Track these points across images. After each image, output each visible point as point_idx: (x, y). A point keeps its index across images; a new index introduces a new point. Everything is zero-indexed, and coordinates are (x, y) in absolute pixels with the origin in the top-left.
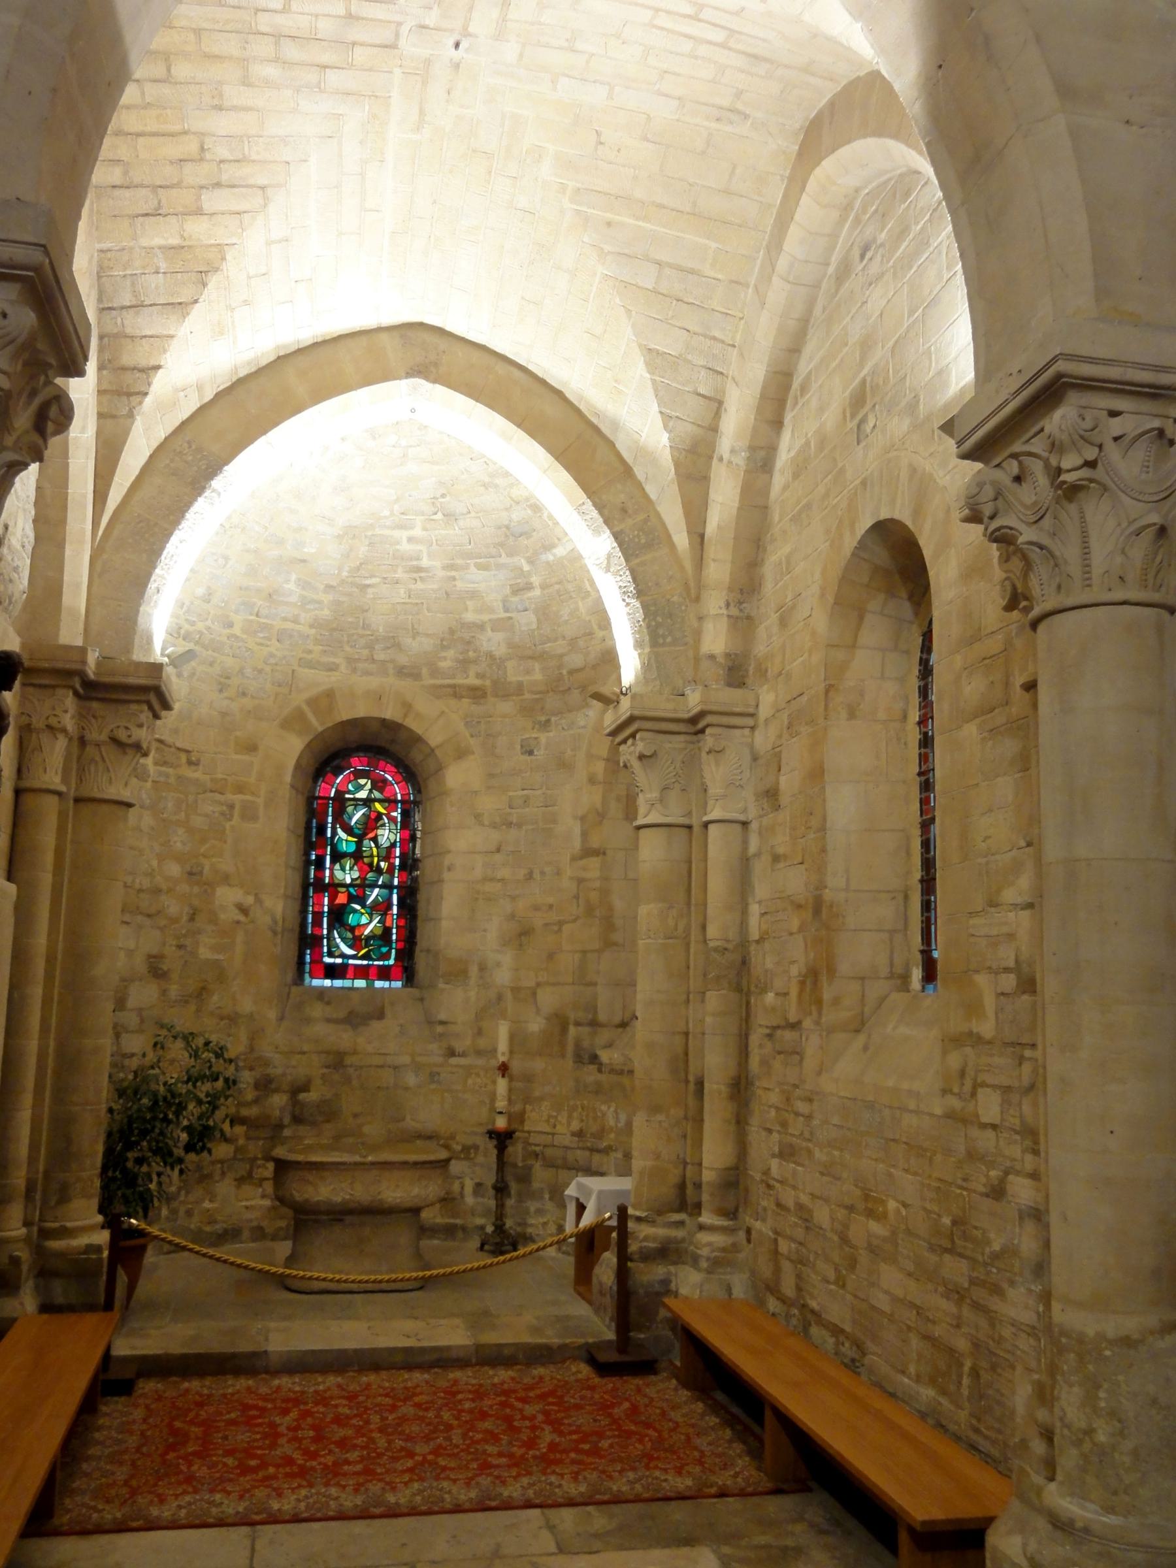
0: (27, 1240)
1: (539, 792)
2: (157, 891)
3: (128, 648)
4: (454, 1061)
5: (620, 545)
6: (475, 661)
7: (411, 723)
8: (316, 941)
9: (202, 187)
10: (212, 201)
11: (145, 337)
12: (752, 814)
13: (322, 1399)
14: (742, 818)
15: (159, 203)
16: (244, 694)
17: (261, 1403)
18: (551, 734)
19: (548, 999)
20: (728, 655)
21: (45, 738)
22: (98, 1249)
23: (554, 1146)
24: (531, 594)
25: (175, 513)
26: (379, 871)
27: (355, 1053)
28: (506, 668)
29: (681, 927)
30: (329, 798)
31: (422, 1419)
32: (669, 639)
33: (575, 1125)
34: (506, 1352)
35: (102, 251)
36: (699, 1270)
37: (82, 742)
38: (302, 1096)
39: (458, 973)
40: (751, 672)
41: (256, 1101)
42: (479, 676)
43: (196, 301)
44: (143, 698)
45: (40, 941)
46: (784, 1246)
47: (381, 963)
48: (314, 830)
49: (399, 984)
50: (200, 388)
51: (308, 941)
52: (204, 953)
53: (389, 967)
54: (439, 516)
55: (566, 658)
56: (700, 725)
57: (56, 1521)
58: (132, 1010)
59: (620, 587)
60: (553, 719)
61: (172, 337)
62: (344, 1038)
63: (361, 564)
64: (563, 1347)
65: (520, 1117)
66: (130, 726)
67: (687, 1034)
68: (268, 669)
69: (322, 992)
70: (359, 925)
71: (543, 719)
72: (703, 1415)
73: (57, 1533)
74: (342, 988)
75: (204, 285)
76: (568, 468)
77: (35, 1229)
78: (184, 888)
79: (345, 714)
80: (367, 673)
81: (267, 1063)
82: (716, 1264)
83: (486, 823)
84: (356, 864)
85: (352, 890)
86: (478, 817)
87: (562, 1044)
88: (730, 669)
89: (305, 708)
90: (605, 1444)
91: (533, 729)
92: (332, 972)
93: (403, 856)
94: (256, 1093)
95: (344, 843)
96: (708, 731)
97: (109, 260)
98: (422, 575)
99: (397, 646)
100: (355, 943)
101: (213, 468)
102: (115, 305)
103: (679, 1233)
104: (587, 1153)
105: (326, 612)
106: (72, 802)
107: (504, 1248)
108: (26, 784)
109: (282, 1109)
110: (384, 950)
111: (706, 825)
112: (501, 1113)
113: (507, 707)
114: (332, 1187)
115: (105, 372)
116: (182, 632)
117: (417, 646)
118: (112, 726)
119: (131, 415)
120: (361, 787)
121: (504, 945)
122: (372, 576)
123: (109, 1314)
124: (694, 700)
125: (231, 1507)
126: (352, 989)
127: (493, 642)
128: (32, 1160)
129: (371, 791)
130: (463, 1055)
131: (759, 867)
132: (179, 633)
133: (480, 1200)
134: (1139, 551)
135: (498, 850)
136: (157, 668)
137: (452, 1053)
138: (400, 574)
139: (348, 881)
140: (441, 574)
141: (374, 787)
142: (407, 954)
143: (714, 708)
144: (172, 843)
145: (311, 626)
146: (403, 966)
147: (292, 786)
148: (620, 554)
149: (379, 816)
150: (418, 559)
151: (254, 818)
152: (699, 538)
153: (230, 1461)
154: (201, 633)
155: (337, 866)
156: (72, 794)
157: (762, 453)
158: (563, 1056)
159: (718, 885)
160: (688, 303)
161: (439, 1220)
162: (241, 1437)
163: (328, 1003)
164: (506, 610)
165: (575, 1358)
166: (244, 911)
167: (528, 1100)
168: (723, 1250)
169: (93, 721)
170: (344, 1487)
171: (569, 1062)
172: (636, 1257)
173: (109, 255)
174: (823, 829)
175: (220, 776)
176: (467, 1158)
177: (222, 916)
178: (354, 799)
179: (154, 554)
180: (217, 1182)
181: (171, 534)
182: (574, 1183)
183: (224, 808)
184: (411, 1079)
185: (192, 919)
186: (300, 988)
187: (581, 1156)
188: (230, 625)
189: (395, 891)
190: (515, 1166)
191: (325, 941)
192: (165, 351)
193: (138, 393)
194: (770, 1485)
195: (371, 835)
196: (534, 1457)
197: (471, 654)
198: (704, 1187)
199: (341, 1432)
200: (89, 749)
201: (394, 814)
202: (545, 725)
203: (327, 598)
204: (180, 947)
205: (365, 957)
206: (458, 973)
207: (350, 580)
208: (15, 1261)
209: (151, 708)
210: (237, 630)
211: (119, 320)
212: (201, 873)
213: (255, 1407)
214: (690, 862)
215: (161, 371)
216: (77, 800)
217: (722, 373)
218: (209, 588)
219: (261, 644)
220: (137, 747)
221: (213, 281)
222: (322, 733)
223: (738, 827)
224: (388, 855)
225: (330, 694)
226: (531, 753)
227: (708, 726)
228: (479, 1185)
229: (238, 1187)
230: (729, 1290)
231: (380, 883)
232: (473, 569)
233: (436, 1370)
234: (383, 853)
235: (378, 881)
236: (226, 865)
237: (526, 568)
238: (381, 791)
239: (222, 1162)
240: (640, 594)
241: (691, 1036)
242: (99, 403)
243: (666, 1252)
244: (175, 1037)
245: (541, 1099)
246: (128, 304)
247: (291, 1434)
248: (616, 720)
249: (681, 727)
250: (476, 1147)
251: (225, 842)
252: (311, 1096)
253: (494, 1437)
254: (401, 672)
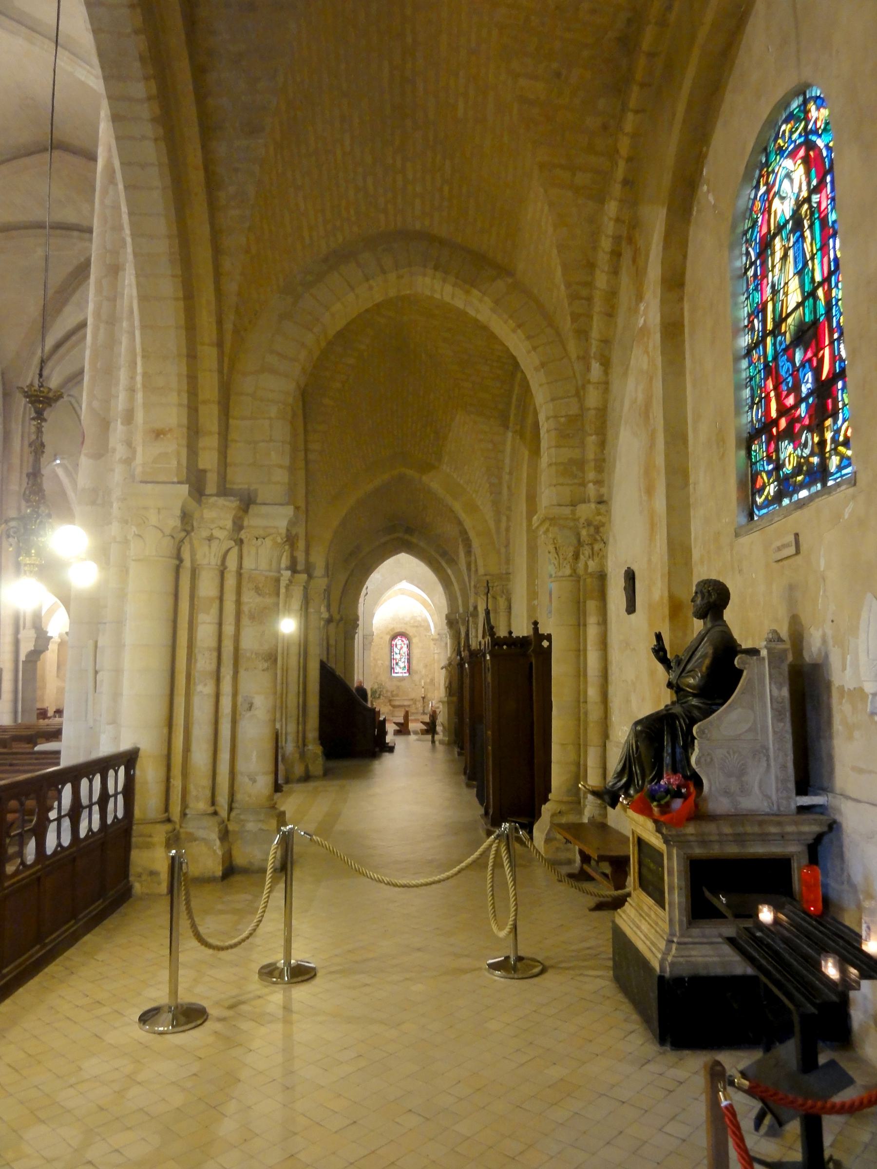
7: (407, 632)
8: (394, 668)
62: (399, 684)
92: (396, 673)
100: (400, 668)
137: (416, 685)
166: (382, 664)
206: (416, 672)
252: (394, 693)
254: (405, 624)
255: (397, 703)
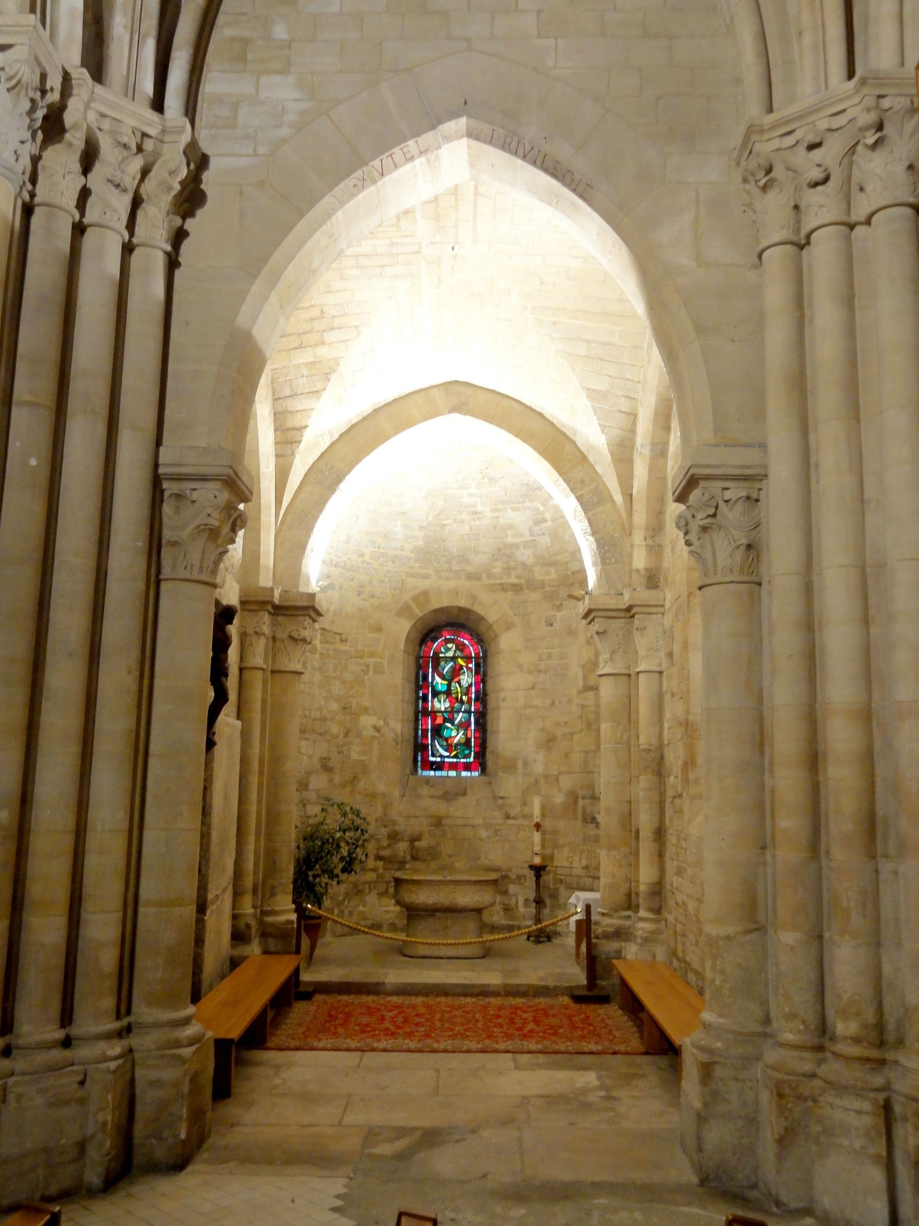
0: (254, 915)
1: (557, 650)
2: (324, 719)
3: (297, 585)
4: (510, 822)
5: (581, 504)
6: (514, 568)
7: (477, 609)
8: (424, 748)
9: (324, 331)
10: (329, 337)
11: (298, 411)
12: (664, 667)
13: (413, 1007)
14: (659, 669)
15: (302, 341)
16: (373, 596)
17: (379, 1007)
18: (564, 613)
19: (566, 782)
20: (646, 570)
21: (254, 639)
22: (292, 922)
23: (571, 875)
24: (545, 525)
25: (320, 505)
26: (462, 702)
27: (448, 817)
28: (534, 571)
29: (625, 737)
30: (430, 657)
31: (463, 1017)
32: (613, 560)
33: (584, 863)
34: (522, 989)
35: (273, 370)
36: (636, 943)
37: (274, 639)
38: (416, 843)
39: (511, 767)
40: (662, 579)
41: (389, 846)
42: (517, 577)
43: (325, 389)
44: (305, 613)
45: (255, 751)
46: (679, 927)
47: (465, 760)
48: (421, 678)
49: (475, 774)
50: (331, 434)
51: (420, 748)
52: (354, 756)
53: (470, 763)
54: (486, 480)
55: (570, 565)
56: (632, 613)
57: (268, 1045)
58: (312, 791)
59: (582, 529)
60: (564, 603)
61: (313, 409)
62: (441, 808)
63: (440, 512)
64: (556, 987)
65: (551, 858)
66: (299, 629)
67: (630, 802)
68: (387, 580)
69: (428, 780)
70: (450, 737)
71: (558, 603)
72: (625, 1022)
73: (268, 1049)
74: (441, 777)
75: (329, 380)
76: (547, 459)
77: (259, 911)
78: (340, 717)
79: (436, 605)
80: (448, 578)
81: (394, 823)
82: (646, 940)
83: (525, 670)
84: (447, 697)
85: (445, 714)
86: (520, 667)
87: (575, 811)
88: (649, 578)
89: (410, 602)
90: (561, 1031)
91: (552, 609)
93: (477, 692)
94: (388, 842)
95: (440, 685)
96: (636, 616)
97: (277, 374)
98: (479, 516)
99: (464, 560)
100: (449, 748)
101: (339, 479)
102: (282, 396)
103: (627, 923)
104: (591, 880)
105: (421, 543)
106: (270, 674)
107: (540, 939)
108: (245, 664)
109: (405, 852)
110: (467, 752)
111: (638, 673)
112: (537, 854)
113: (536, 596)
114: (426, 894)
115: (278, 432)
116: (334, 562)
117: (478, 560)
118: (290, 630)
119: (293, 454)
120: (448, 650)
121: (538, 748)
122: (447, 519)
123: (297, 956)
124: (627, 599)
125: (353, 1044)
126: (448, 777)
127: (525, 555)
128: (256, 872)
129: (455, 651)
130: (515, 818)
131: (667, 698)
132: (332, 564)
133: (529, 909)
134: (739, 556)
135: (533, 688)
136: (312, 596)
137: (508, 817)
138: (465, 516)
139: (443, 709)
140: (489, 514)
141: (457, 648)
142: (481, 756)
143: (637, 603)
144: (332, 690)
145: (412, 552)
146: (479, 763)
147: (404, 652)
148: (581, 509)
149: (461, 667)
150: (475, 506)
151: (383, 672)
152: (629, 497)
153: (357, 1028)
154: (345, 562)
155: (436, 700)
156: (270, 669)
157: (660, 447)
158: (576, 818)
159: (644, 711)
160: (608, 361)
161: (504, 922)
162: (365, 1020)
163: (432, 786)
164: (532, 535)
165: (563, 995)
166: (377, 729)
167: (555, 846)
168: (651, 932)
169: (279, 627)
170: (412, 1041)
171: (579, 822)
172: (601, 936)
173: (277, 371)
174: (688, 679)
175: (360, 648)
176: (520, 883)
177: (365, 733)
178: (445, 657)
179: (309, 530)
180: (367, 895)
181: (318, 518)
182: (574, 896)
183: (363, 667)
184: (483, 834)
185: (346, 735)
186: (415, 777)
187: (588, 881)
188: (363, 555)
189: (472, 714)
190: (549, 888)
191: (430, 747)
192: (309, 417)
193: (296, 442)
194: (644, 1050)
195: (456, 680)
196: (519, 1035)
197: (512, 563)
198: (641, 895)
199: (417, 1020)
200: (278, 643)
201: (470, 666)
202: (559, 607)
203: (421, 534)
204: (340, 752)
205: (456, 756)
206: (511, 767)
207: (434, 522)
208: (248, 926)
209: (311, 617)
210: (367, 558)
211: (284, 404)
212: (351, 707)
213: (375, 1008)
214: (630, 696)
215: (308, 428)
216: (273, 672)
217: (634, 399)
218: (348, 535)
219: (382, 565)
220: (304, 640)
221: (333, 377)
222: (421, 617)
223: (657, 675)
224: (467, 692)
225: (425, 593)
226: (551, 625)
227: (635, 614)
228: (527, 900)
229: (380, 898)
230: (654, 957)
231: (463, 710)
232: (509, 511)
233: (480, 997)
234: (464, 691)
235: (461, 708)
236: (366, 702)
237: (542, 508)
238: (462, 651)
239: (369, 883)
240: (594, 533)
241: (632, 803)
242: (276, 449)
243: (619, 934)
244: (332, 805)
245: (563, 846)
246: (288, 395)
247: (391, 1020)
248: (584, 610)
249: (622, 614)
250: (525, 876)
251: (365, 688)
253: (501, 1026)
254: (469, 577)
255: (423, 897)
